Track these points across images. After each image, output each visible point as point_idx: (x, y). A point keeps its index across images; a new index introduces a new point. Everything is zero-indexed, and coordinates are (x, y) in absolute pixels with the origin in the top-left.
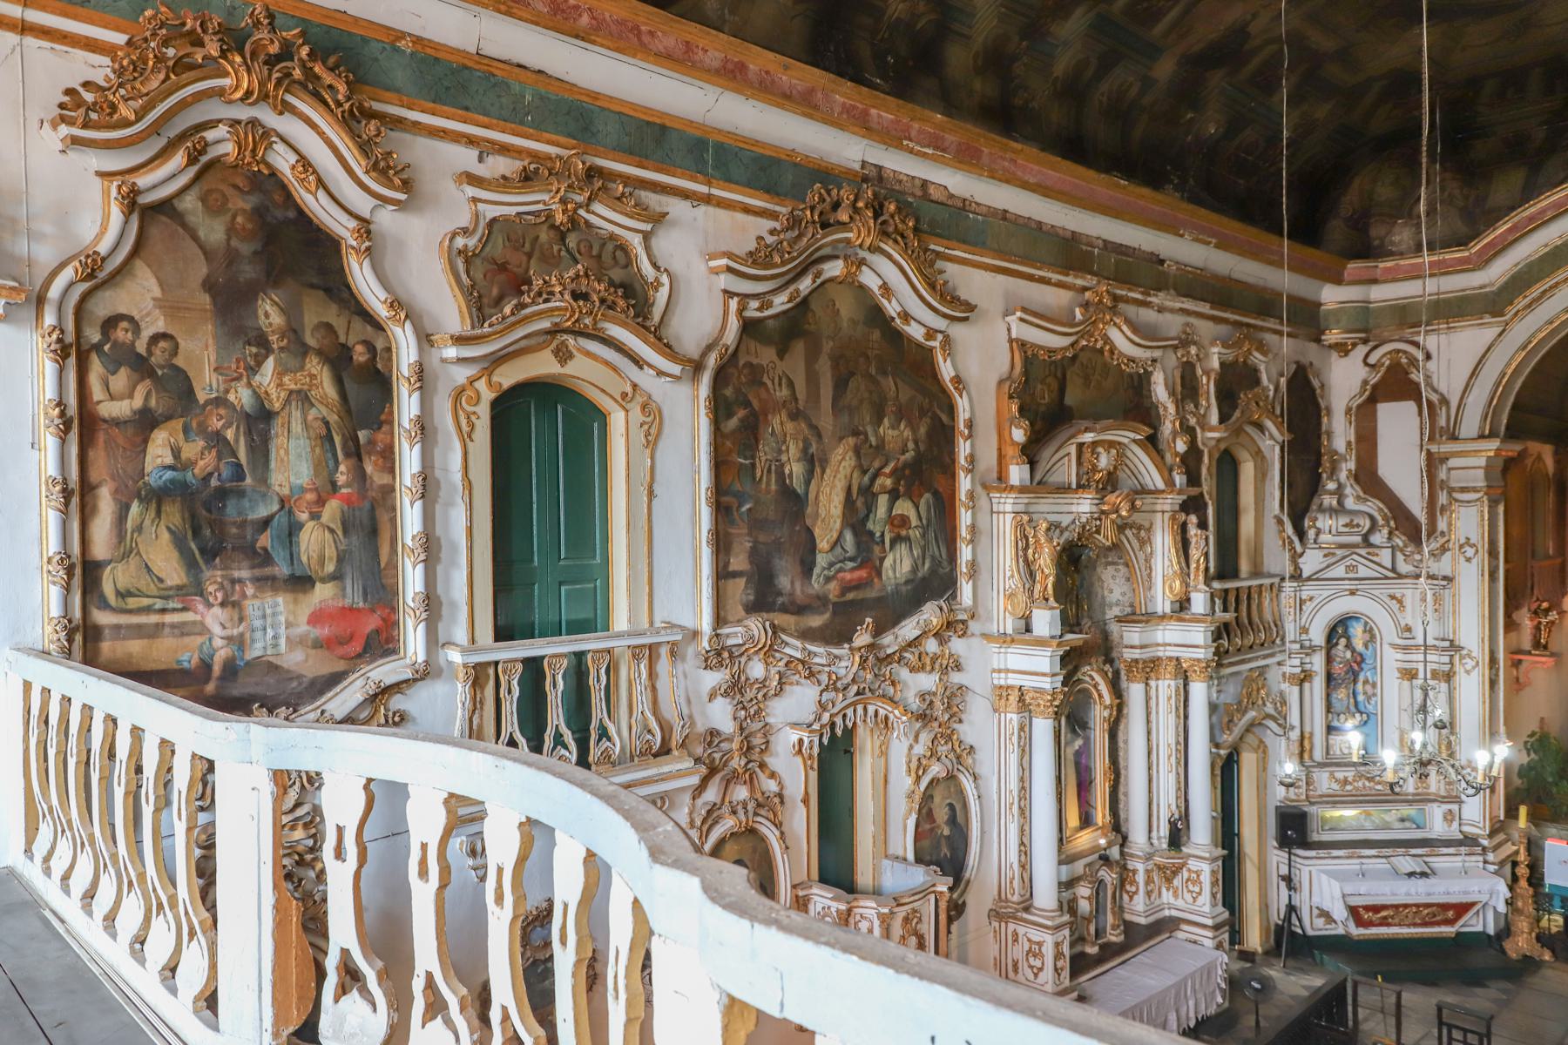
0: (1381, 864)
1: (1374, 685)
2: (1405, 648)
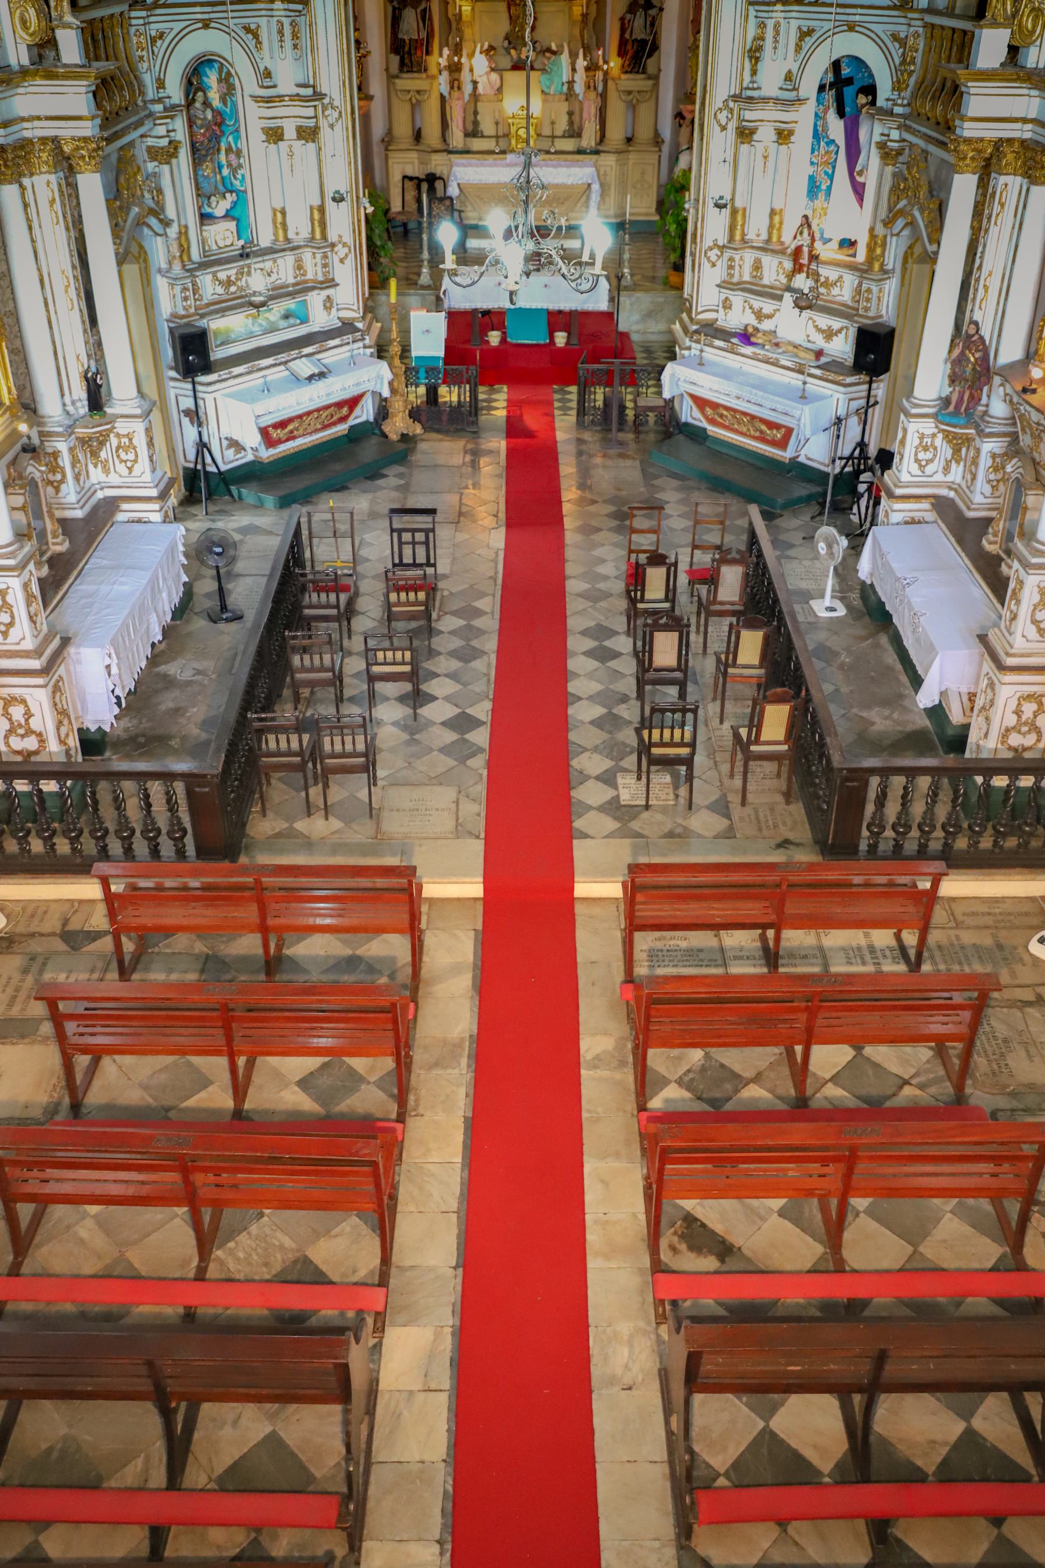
0: (278, 374)
1: (239, 153)
2: (268, 100)
